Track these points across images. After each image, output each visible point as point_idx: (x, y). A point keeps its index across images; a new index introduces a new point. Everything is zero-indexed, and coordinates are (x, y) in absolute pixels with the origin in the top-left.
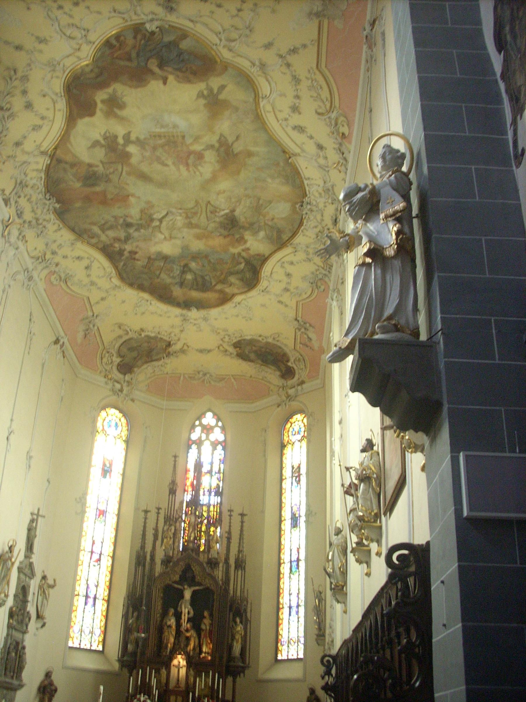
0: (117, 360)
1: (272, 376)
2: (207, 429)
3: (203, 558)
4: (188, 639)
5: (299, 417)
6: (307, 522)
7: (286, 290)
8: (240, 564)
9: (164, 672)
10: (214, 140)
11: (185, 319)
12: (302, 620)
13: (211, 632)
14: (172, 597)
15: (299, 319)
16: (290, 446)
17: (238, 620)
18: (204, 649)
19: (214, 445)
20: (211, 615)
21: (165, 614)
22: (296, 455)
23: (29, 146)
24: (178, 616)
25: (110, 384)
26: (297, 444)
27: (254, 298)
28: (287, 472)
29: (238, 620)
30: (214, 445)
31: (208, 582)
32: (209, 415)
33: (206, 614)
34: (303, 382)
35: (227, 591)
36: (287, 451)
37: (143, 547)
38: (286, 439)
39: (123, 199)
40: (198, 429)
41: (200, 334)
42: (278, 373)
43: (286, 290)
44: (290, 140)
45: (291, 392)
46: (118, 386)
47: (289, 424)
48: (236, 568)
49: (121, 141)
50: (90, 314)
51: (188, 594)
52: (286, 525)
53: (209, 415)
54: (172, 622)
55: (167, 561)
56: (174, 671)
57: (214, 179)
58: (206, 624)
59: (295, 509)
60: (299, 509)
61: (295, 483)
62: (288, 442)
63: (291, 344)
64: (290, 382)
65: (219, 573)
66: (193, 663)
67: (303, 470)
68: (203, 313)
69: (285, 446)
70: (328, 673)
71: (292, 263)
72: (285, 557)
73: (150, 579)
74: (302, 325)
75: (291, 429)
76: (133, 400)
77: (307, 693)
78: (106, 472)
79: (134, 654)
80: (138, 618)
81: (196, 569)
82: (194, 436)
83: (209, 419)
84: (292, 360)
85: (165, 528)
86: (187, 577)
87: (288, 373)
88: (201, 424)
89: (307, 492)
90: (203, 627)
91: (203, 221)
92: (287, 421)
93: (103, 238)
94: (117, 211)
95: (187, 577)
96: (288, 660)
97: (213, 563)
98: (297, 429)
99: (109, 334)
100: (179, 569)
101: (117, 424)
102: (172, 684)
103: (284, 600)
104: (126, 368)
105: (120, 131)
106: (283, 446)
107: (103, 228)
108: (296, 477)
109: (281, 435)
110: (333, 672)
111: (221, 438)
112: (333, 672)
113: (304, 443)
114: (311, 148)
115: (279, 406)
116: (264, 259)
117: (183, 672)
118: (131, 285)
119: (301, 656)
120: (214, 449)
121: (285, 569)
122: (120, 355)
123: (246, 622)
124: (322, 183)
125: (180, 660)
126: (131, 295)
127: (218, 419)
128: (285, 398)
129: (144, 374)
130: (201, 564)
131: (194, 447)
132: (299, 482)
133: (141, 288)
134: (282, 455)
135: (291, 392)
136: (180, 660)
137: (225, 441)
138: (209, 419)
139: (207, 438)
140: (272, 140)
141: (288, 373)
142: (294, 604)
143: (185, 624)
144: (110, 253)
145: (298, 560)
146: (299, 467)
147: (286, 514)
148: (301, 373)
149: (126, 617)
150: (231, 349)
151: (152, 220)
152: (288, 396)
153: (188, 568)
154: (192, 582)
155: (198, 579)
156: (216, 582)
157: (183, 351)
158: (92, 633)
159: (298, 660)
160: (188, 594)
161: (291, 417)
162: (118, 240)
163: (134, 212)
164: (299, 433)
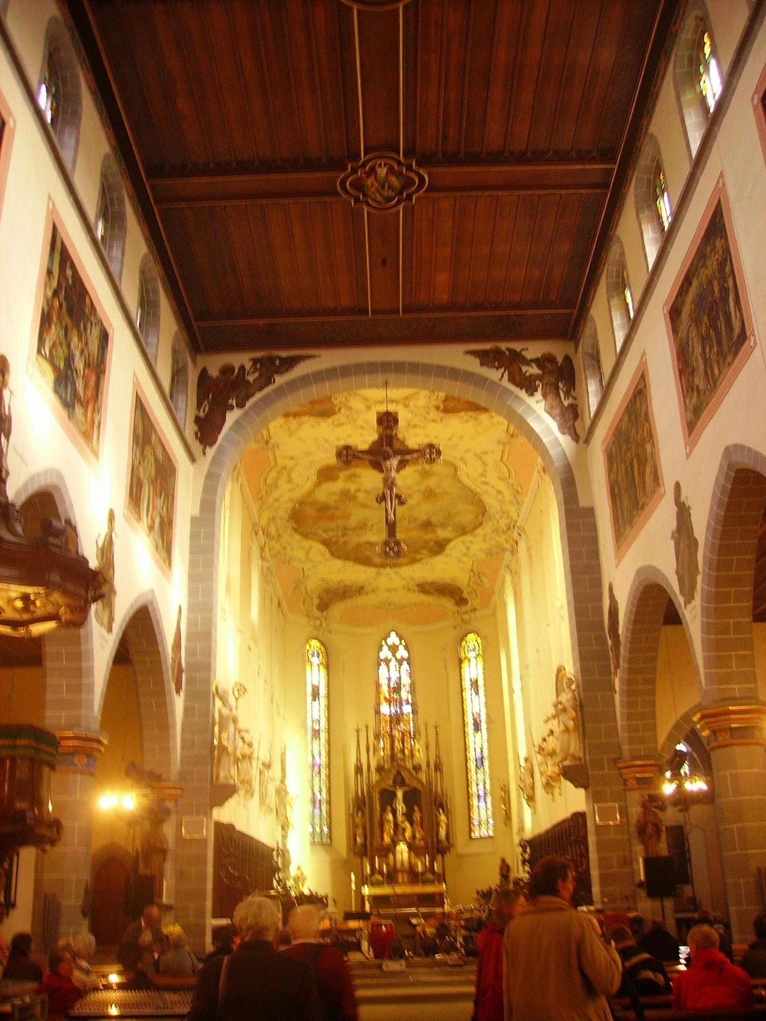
0: (316, 601)
1: (448, 604)
2: (394, 649)
3: (409, 765)
4: (404, 830)
5: (471, 637)
6: (488, 729)
7: (465, 555)
8: (438, 767)
9: (391, 856)
10: (422, 488)
11: (378, 573)
12: (489, 806)
13: (422, 823)
14: (388, 797)
15: (475, 569)
16: (466, 661)
17: (441, 811)
18: (418, 835)
20: (421, 811)
21: (383, 811)
22: (473, 670)
23: (282, 500)
24: (394, 812)
25: (312, 622)
26: (473, 661)
27: (439, 560)
28: (467, 684)
29: (441, 811)
30: (400, 662)
31: (415, 784)
32: (393, 634)
33: (416, 808)
34: (475, 610)
35: (431, 789)
36: (465, 665)
37: (359, 760)
38: (463, 655)
39: (348, 516)
40: (385, 648)
41: (393, 582)
42: (453, 601)
43: (465, 555)
44: (478, 488)
45: (466, 617)
46: (318, 622)
48: (436, 770)
49: (352, 490)
50: (301, 575)
51: (400, 794)
52: (470, 728)
53: (393, 634)
54: (390, 817)
55: (380, 769)
56: (398, 856)
57: (418, 504)
58: (417, 816)
60: (479, 715)
61: (474, 694)
63: (466, 582)
64: (464, 609)
65: (423, 776)
66: (411, 847)
67: (481, 683)
68: (394, 570)
70: (525, 851)
71: (471, 542)
72: (471, 755)
73: (369, 786)
74: (476, 574)
76: (330, 632)
77: (499, 862)
78: (315, 695)
79: (364, 845)
80: (362, 816)
81: (405, 774)
82: (382, 655)
83: (393, 639)
84: (465, 592)
86: (400, 781)
87: (461, 601)
89: (486, 703)
90: (414, 818)
91: (406, 523)
92: (463, 639)
93: (324, 536)
94: (340, 523)
95: (400, 781)
96: (481, 838)
97: (417, 768)
98: (471, 647)
99: (312, 584)
100: (391, 776)
102: (398, 865)
103: (474, 789)
104: (324, 606)
105: (352, 487)
106: (461, 661)
107: (325, 531)
109: (458, 652)
110: (528, 850)
111: (405, 654)
112: (528, 850)
113: (480, 660)
114: (494, 492)
115: (455, 627)
116: (449, 541)
117: (406, 855)
118: (340, 557)
119: (491, 833)
121: (472, 765)
122: (320, 598)
123: (447, 814)
124: (499, 508)
125: (402, 847)
126: (338, 563)
127: (401, 639)
128: (459, 622)
129: (338, 609)
130: (408, 770)
131: (383, 664)
132: (477, 693)
133: (348, 558)
134: (460, 668)
135: (466, 617)
136: (402, 847)
137: (409, 658)
138: (393, 639)
140: (464, 486)
141: (461, 601)
142: (481, 793)
143: (400, 818)
144: (326, 543)
145: (482, 758)
146: (477, 681)
147: (469, 720)
148: (473, 602)
149: (351, 817)
150: (416, 589)
151: (366, 525)
152: (462, 620)
153: (399, 773)
154: (402, 783)
155: (407, 781)
156: (422, 783)
157: (373, 591)
158: (322, 830)
159: (490, 837)
160: (400, 794)
162: (337, 536)
163: (353, 522)
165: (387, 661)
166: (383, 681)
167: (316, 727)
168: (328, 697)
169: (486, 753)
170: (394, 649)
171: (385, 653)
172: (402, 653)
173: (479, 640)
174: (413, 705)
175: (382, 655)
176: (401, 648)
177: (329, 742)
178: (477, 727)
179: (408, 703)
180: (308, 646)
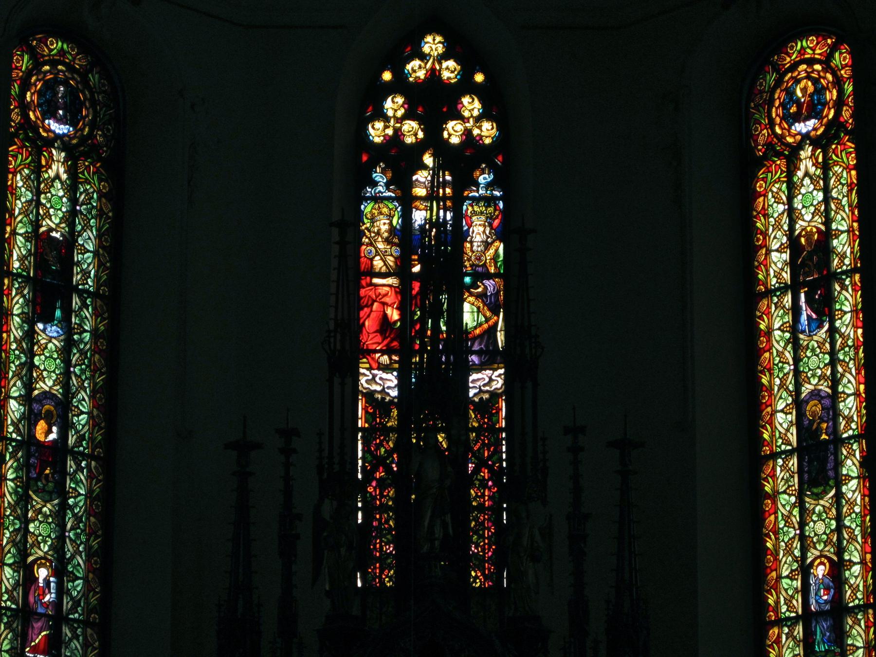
2: (433, 103)
5: (812, 46)
19: (461, 162)
32: (433, 45)
47: (771, 78)
52: (782, 477)
53: (433, 45)
59: (814, 408)
62: (769, 145)
69: (759, 163)
72: (785, 595)
75: (779, 96)
83: (432, 57)
85: (327, 509)
88: (401, 85)
101: (72, 92)
108: (812, 287)
120: (464, 182)
132: (825, 308)
138: (432, 57)
139: (434, 139)
161: (781, 45)
164: (813, 110)
165: (401, 159)
166: (381, 255)
167: (46, 433)
168: (111, 299)
169: (855, 596)
170: (433, 103)
171: (394, 121)
172: (471, 122)
173: (841, 59)
174: (517, 360)
175: (377, 132)
176: (471, 105)
177: (105, 505)
178: (818, 465)
179: (490, 359)
180: (24, 62)
